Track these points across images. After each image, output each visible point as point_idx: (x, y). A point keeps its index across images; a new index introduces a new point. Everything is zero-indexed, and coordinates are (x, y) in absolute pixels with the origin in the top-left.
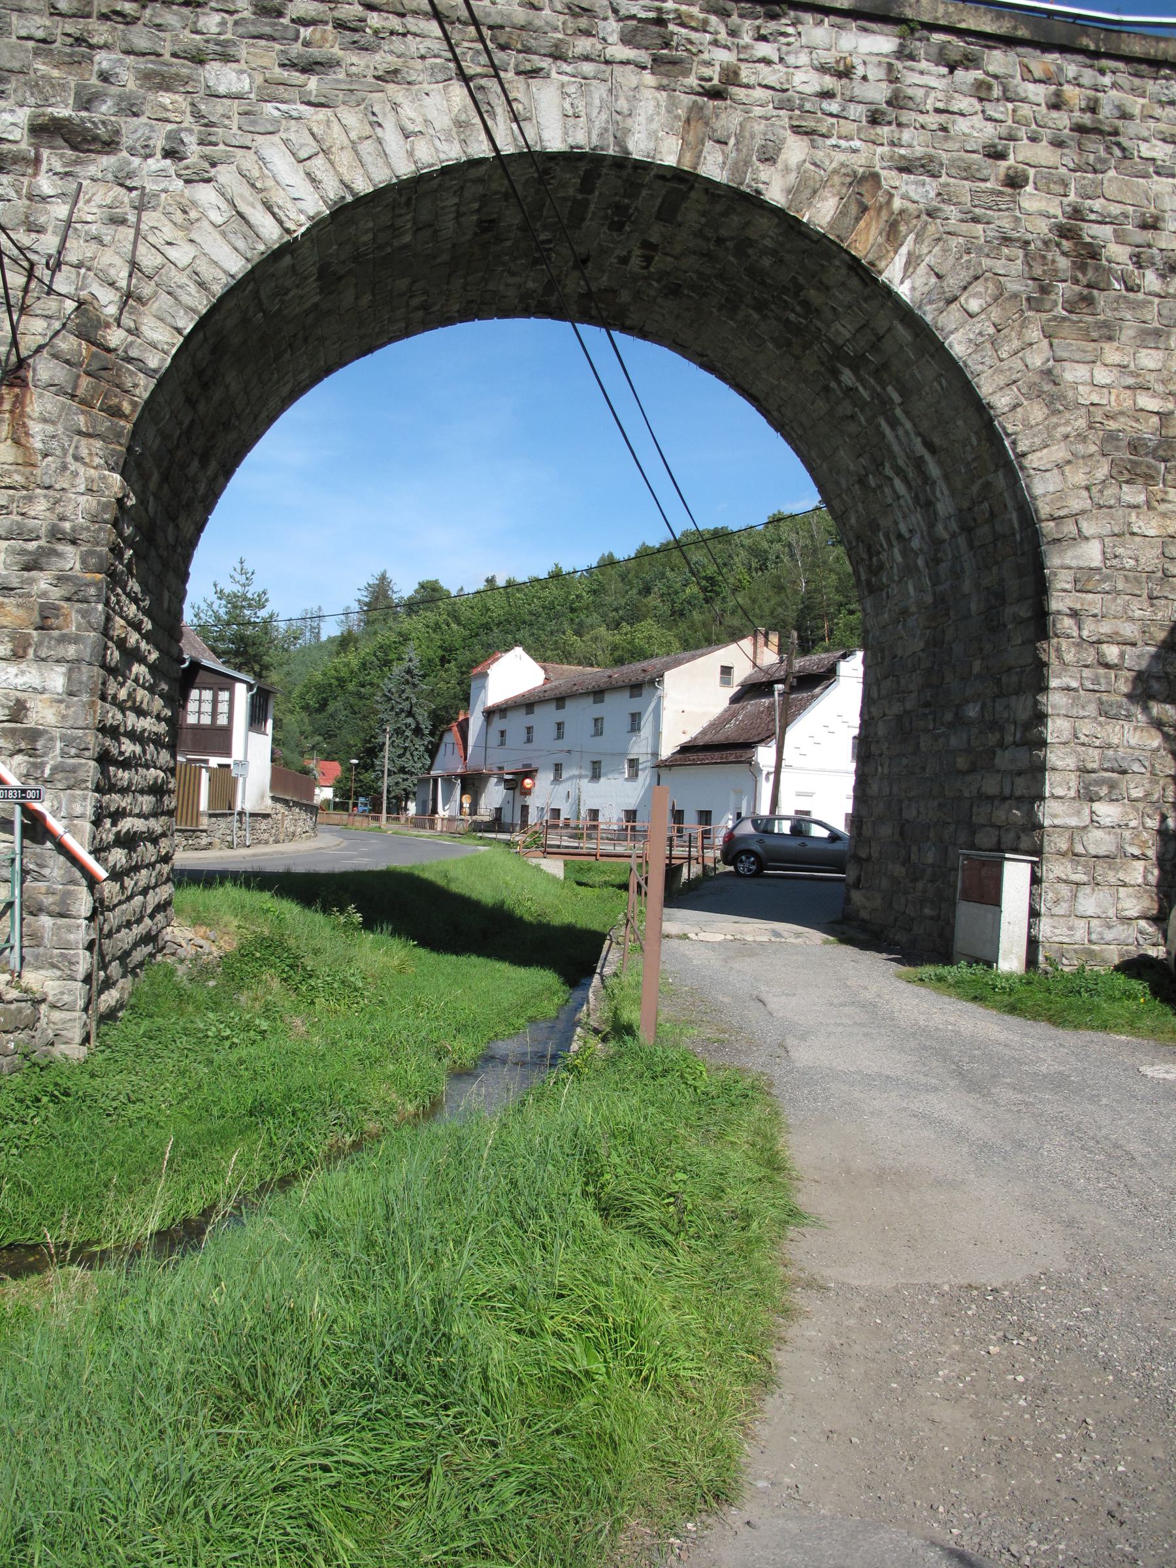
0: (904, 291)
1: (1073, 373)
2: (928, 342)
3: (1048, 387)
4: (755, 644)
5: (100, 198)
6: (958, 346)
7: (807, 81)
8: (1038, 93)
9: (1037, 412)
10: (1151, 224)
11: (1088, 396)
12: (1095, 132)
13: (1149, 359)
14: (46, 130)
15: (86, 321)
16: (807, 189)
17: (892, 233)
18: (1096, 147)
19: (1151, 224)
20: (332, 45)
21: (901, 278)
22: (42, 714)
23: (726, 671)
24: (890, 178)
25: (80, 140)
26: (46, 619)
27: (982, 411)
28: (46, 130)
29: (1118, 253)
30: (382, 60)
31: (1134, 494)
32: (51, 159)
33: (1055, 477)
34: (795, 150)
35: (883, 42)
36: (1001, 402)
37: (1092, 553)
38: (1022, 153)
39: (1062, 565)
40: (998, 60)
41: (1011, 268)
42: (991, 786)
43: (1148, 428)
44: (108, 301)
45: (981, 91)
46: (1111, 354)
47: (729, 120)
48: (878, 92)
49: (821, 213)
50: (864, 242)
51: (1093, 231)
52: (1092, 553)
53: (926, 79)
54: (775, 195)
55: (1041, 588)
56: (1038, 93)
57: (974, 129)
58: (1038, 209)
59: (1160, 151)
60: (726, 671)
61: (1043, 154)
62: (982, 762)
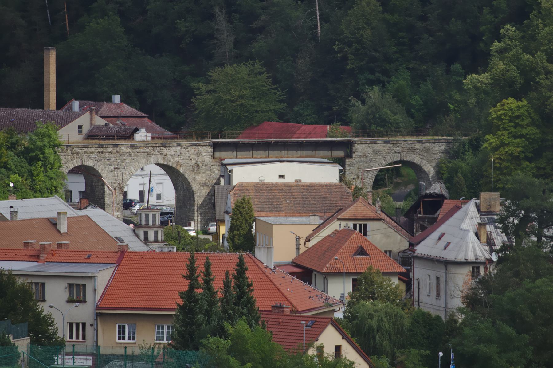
0: (182, 172)
1: (197, 177)
2: (183, 175)
3: (194, 179)
4: (91, 114)
5: (120, 173)
6: (186, 176)
7: (173, 153)
8: (193, 150)
9: (193, 181)
10: (204, 161)
11: (198, 179)
12: (199, 153)
13: (204, 175)
14: (115, 168)
15: (119, 184)
16: (173, 164)
17: (181, 166)
18: (199, 155)
19: (204, 161)
20: (135, 157)
21: (181, 171)
22: (119, 216)
23: (80, 127)
24: (180, 161)
25: (117, 168)
26: (119, 209)
27: (189, 182)
28: (115, 168)
29: (201, 165)
30: (139, 157)
31: (202, 188)
32: (116, 170)
33: (195, 187)
34: (172, 160)
35: (179, 148)
36: (190, 181)
37: (198, 194)
38: (192, 157)
39: (196, 196)
40: (189, 147)
41: (191, 168)
42: (190, 215)
43: (204, 182)
44: (121, 182)
45: (188, 151)
46: (200, 175)
47: (166, 158)
48: (179, 153)
49: (174, 166)
50: (178, 168)
51: (199, 163)
52: (198, 194)
53: (183, 151)
54: (171, 165)
55: (194, 198)
56: (193, 150)
57: (188, 155)
58: (193, 162)
59: (205, 154)
60: (80, 127)
61: (194, 156)
62: (189, 212)
